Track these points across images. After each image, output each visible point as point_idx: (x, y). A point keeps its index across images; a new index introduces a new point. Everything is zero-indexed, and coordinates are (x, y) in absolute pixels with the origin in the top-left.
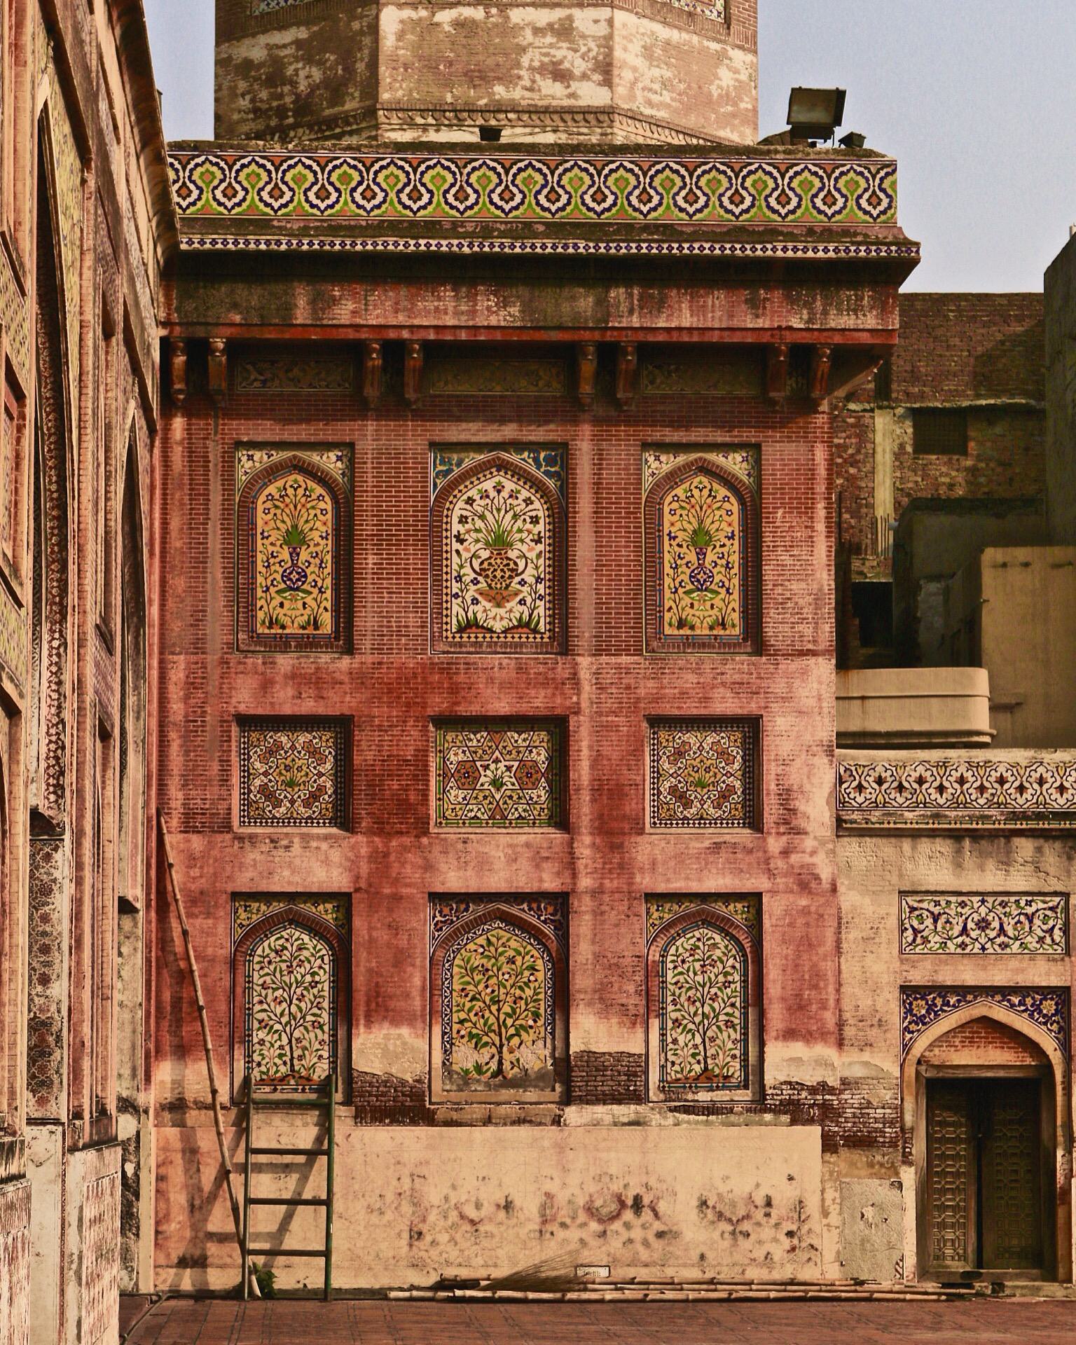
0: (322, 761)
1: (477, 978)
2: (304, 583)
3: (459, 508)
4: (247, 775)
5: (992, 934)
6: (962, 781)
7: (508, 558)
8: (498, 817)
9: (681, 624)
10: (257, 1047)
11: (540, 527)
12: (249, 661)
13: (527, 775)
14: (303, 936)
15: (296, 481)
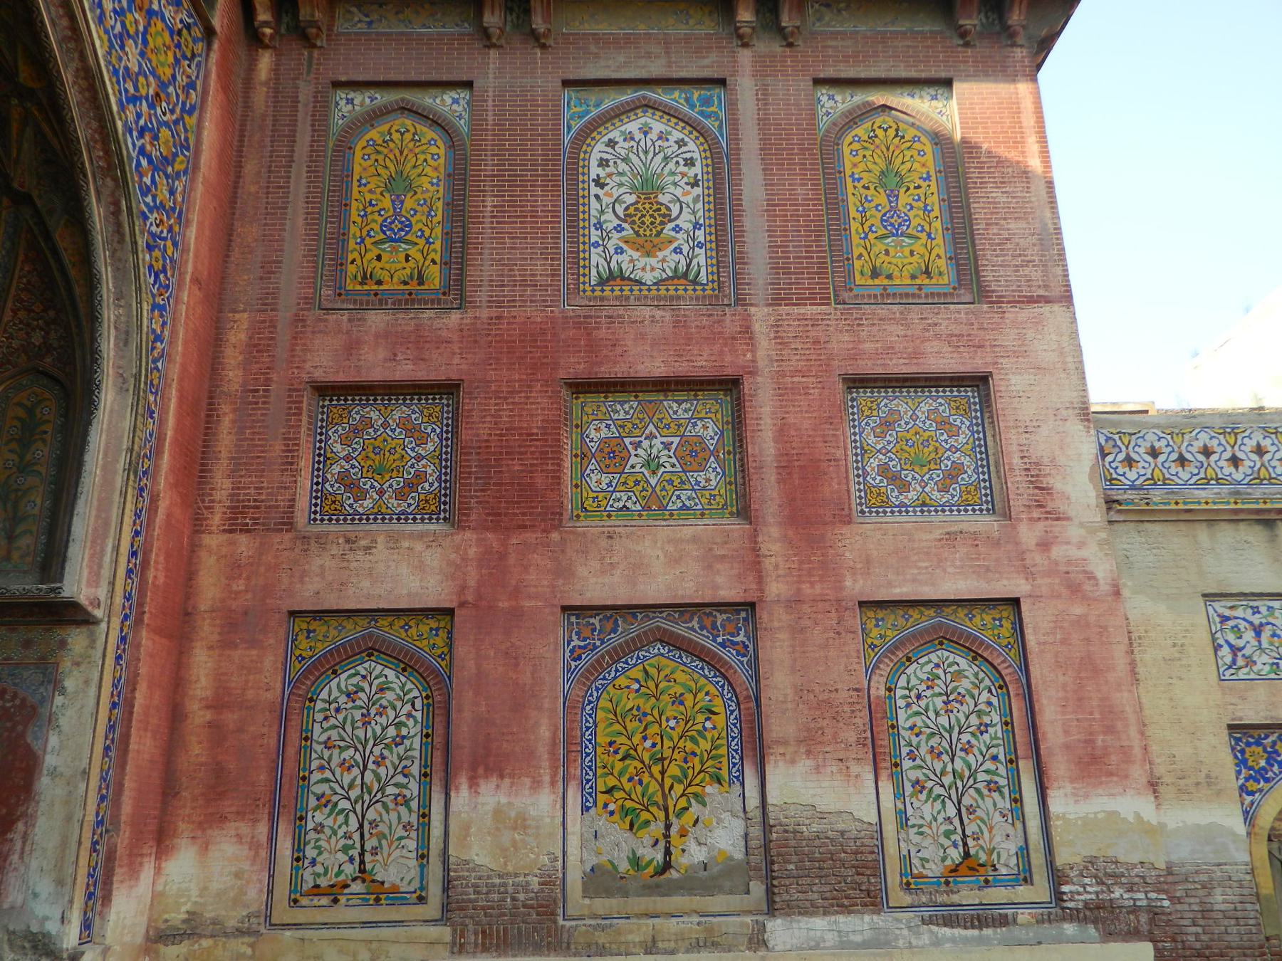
0: (422, 442)
1: (630, 726)
2: (407, 233)
3: (598, 150)
4: (323, 459)
7: (658, 203)
8: (654, 507)
10: (312, 835)
11: (697, 169)
12: (332, 317)
13: (693, 455)
14: (387, 671)
15: (403, 125)
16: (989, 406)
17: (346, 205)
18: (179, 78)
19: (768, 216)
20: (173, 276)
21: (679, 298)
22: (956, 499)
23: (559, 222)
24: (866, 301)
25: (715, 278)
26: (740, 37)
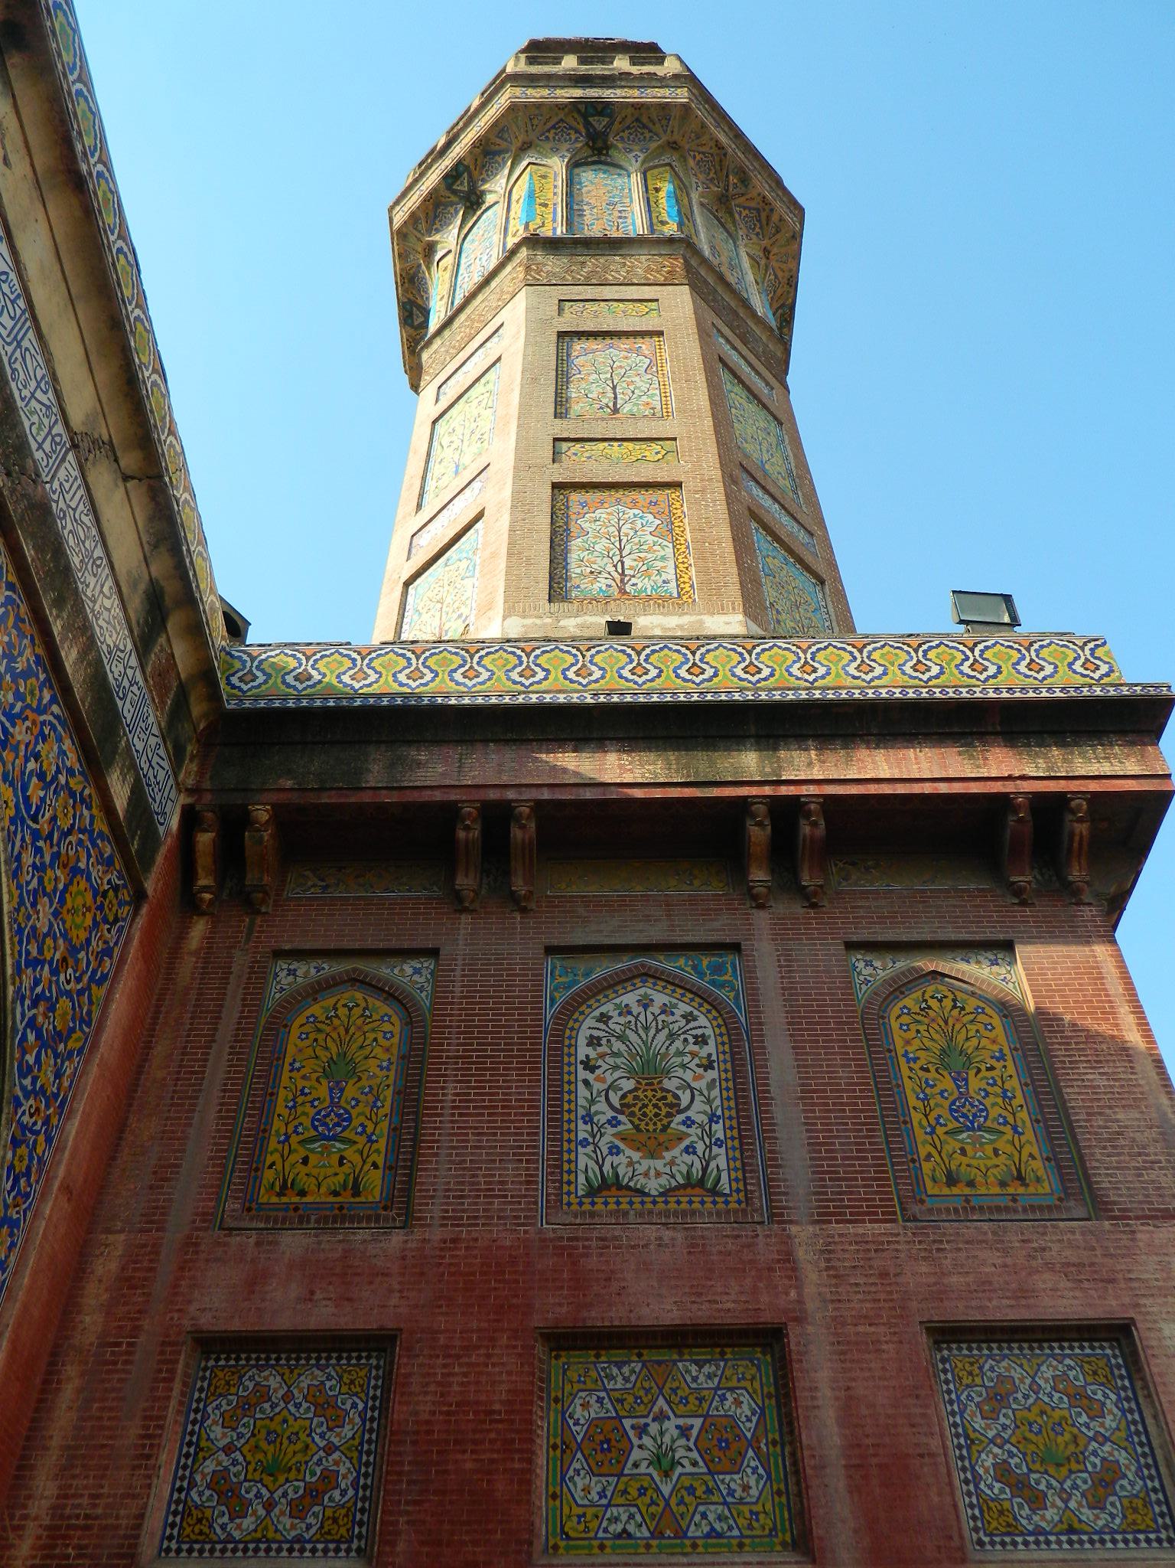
0: (337, 1422)
2: (345, 1129)
3: (588, 1026)
4: (195, 1450)
7: (663, 1090)
9: (952, 1180)
11: (711, 1048)
12: (235, 1240)
16: (1140, 1370)
17: (272, 1094)
18: (94, 943)
19: (805, 1105)
20: (37, 1182)
21: (693, 1213)
22: (1118, 1521)
23: (538, 1114)
24: (944, 1217)
25: (741, 1186)
26: (754, 898)
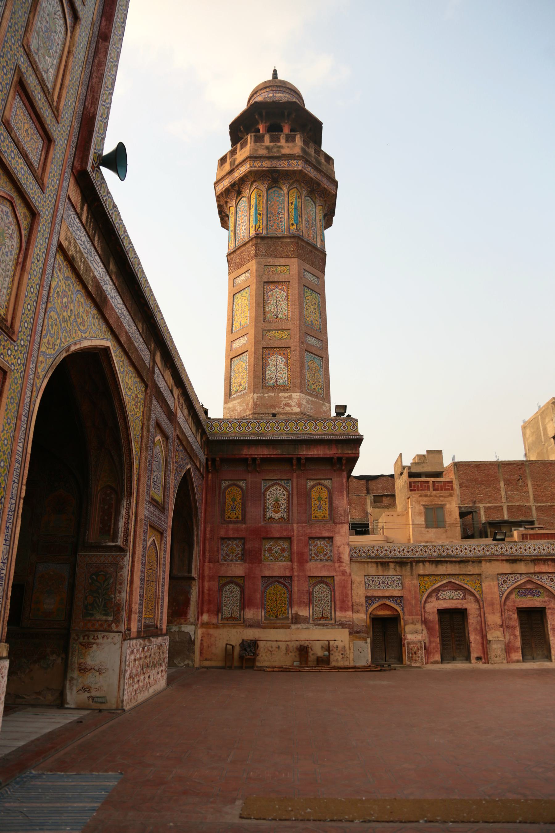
0: (239, 547)
3: (268, 493)
5: (385, 585)
6: (377, 550)
8: (276, 559)
11: (285, 497)
13: (283, 550)
